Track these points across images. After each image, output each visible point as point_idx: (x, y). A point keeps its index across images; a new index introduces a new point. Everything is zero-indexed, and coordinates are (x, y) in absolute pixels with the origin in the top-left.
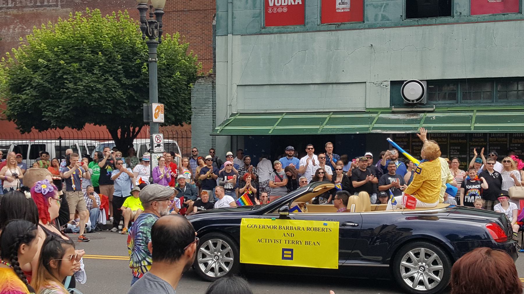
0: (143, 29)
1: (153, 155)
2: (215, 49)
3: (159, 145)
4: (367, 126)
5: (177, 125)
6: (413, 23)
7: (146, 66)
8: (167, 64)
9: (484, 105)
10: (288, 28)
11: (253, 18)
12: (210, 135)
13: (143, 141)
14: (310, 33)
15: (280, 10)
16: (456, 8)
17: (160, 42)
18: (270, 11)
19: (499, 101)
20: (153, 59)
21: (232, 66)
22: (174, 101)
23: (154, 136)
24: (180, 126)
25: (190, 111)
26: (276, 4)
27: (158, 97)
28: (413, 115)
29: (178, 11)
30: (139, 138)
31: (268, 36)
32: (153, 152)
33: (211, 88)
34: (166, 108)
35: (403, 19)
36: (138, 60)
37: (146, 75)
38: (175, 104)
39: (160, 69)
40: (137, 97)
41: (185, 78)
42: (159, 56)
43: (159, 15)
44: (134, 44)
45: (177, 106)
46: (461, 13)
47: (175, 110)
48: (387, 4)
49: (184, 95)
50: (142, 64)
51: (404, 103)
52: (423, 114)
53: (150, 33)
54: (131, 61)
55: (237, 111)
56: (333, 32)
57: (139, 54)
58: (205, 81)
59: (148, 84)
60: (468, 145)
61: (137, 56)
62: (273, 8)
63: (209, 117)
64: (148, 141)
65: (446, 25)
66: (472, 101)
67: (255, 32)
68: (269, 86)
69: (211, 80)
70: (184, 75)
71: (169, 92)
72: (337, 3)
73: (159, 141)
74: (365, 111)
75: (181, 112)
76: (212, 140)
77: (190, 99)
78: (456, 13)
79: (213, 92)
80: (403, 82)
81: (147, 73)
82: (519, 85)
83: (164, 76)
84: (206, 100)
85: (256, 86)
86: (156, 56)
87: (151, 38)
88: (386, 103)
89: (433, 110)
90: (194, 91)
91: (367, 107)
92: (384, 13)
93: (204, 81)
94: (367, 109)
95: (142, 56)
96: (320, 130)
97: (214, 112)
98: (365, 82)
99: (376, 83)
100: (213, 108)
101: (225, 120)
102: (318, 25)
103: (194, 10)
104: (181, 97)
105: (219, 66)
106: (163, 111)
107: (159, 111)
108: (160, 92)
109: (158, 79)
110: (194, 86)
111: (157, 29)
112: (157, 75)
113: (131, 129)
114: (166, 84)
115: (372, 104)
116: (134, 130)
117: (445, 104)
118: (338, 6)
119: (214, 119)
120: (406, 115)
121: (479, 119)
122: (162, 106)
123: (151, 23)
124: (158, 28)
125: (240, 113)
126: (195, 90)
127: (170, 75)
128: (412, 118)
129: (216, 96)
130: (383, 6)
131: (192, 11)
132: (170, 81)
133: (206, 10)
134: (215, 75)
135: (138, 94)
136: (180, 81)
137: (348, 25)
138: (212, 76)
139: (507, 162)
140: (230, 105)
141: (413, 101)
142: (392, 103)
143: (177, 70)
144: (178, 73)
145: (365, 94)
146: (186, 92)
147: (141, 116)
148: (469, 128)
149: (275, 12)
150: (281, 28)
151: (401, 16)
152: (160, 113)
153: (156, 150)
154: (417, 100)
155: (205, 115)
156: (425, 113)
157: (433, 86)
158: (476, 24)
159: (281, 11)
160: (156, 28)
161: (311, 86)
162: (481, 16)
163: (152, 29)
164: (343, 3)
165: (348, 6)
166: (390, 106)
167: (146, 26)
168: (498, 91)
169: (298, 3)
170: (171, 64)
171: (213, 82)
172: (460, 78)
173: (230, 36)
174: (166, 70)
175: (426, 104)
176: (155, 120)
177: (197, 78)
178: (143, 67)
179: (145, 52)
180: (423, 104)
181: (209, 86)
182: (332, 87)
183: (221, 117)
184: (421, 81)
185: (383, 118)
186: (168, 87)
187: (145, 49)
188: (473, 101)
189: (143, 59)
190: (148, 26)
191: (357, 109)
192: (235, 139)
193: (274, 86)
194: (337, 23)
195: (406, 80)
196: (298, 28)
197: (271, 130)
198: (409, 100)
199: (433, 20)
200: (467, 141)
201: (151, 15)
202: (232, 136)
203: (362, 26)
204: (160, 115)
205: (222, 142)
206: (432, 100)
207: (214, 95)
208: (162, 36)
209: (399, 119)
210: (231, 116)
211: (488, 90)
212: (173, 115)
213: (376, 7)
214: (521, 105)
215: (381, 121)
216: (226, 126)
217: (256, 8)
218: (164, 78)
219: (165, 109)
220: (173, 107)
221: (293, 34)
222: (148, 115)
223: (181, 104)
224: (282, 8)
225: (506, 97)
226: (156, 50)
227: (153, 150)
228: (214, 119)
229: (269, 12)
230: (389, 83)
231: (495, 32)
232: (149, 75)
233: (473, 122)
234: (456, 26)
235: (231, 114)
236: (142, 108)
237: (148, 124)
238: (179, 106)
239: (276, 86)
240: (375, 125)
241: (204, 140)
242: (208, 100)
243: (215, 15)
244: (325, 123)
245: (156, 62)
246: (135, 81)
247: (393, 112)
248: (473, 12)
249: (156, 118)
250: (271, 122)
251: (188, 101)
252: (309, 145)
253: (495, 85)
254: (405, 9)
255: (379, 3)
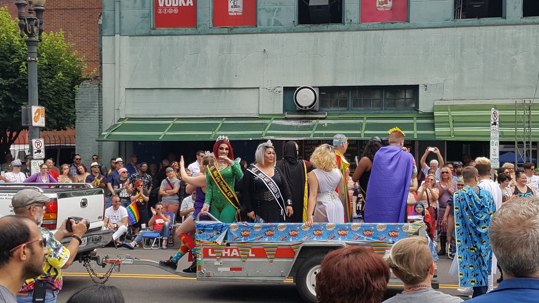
0: (21, 26)
1: (32, 161)
2: (101, 50)
3: (39, 151)
4: (260, 132)
5: (59, 130)
6: (305, 29)
7: (25, 66)
8: (48, 64)
9: (374, 113)
10: (179, 30)
11: (142, 18)
12: (96, 141)
13: (22, 147)
14: (203, 36)
15: (170, 11)
16: (347, 14)
17: (40, 40)
18: (160, 11)
19: (388, 108)
20: (33, 58)
21: (120, 69)
22: (56, 104)
23: (34, 141)
24: (62, 130)
25: (74, 115)
26: (167, 5)
27: (38, 98)
28: (305, 121)
29: (60, 9)
30: (17, 144)
31: (158, 37)
32: (33, 159)
33: (98, 91)
34: (47, 111)
35: (296, 25)
36: (16, 59)
37: (25, 75)
38: (57, 107)
39: (40, 69)
40: (15, 99)
41: (68, 79)
42: (39, 55)
43: (39, 12)
44: (12, 42)
45: (60, 109)
46: (351, 20)
47: (58, 114)
48: (280, 9)
49: (67, 97)
50: (20, 63)
51: (297, 109)
52: (315, 121)
53: (30, 31)
54: (8, 61)
55: (126, 116)
56: (226, 36)
57: (18, 53)
58: (91, 83)
59: (27, 85)
60: (359, 152)
61: (15, 55)
62: (163, 9)
63: (95, 121)
64: (27, 147)
65: (337, 33)
66: (362, 109)
67: (144, 32)
68: (159, 90)
69: (97, 82)
70: (68, 77)
71: (51, 94)
72: (230, 6)
73: (39, 147)
74: (258, 117)
75: (64, 116)
76: (98, 146)
77: (74, 102)
78: (347, 20)
79: (99, 95)
80: (296, 88)
81: (26, 73)
82: (406, 94)
83: (45, 77)
84: (92, 103)
85: (145, 90)
86: (36, 55)
87: (30, 36)
88: (279, 109)
89: (325, 117)
90: (78, 94)
91: (260, 113)
92: (277, 18)
93: (89, 84)
94: (260, 115)
95: (20, 55)
96: (213, 136)
97: (100, 116)
98: (259, 88)
99: (269, 89)
100: (99, 113)
101: (113, 125)
102: (210, 28)
103: (78, 9)
104: (63, 99)
105: (106, 68)
106: (44, 114)
107: (39, 115)
108: (41, 94)
109: (38, 80)
110: (79, 88)
111: (37, 26)
112: (37, 75)
113: (8, 133)
114: (48, 86)
115: (265, 110)
116: (11, 135)
117: (337, 111)
118: (230, 9)
119: (101, 124)
120: (299, 121)
121: (369, 127)
122: (42, 109)
123: (30, 20)
124: (38, 26)
125: (129, 118)
126: (80, 92)
127: (52, 75)
128: (304, 124)
129: (102, 100)
130: (275, 12)
131: (76, 9)
132: (51, 82)
133: (92, 9)
134: (102, 77)
135: (16, 96)
136: (62, 82)
137: (240, 29)
138: (99, 78)
139: (126, 173)
140: (118, 109)
141: (306, 107)
142: (285, 110)
143: (59, 70)
144: (60, 74)
145: (258, 99)
146: (70, 95)
147: (20, 119)
148: (359, 135)
149: (165, 13)
150: (172, 30)
151: (294, 21)
152: (40, 116)
153: (35, 156)
154: (310, 107)
155: (91, 119)
156: (318, 120)
157: (325, 93)
158: (366, 31)
159: (172, 12)
160: (36, 25)
161: (204, 91)
162: (370, 25)
163: (32, 26)
164: (236, 6)
165: (241, 9)
166: (283, 112)
167: (24, 23)
168: (387, 99)
169: (190, 4)
170: (52, 64)
171: (99, 85)
172: (351, 85)
173: (117, 36)
174: (48, 71)
175: (319, 111)
176: (34, 124)
177: (82, 80)
178: (21, 67)
179: (23, 50)
180: (315, 111)
181: (95, 88)
182: (225, 92)
183: (108, 122)
184: (313, 87)
185: (276, 124)
186: (49, 88)
187: (23, 47)
188: (363, 108)
189: (21, 58)
190: (27, 22)
191: (250, 115)
192: (123, 145)
193: (165, 90)
194: (230, 27)
195: (299, 86)
196: (190, 30)
197: (161, 135)
198: (302, 107)
199: (325, 27)
200: (357, 148)
201: (30, 12)
202: (120, 142)
203: (255, 30)
204: (40, 118)
205: (109, 148)
206: (324, 107)
207: (100, 98)
208: (43, 33)
209: (291, 126)
210: (119, 121)
211: (378, 98)
212: (54, 118)
213: (269, 11)
214: (408, 113)
215: (274, 127)
216: (113, 131)
217: (144, 7)
218: (45, 79)
219: (46, 112)
220: (55, 111)
221: (184, 36)
222: (27, 119)
223: (64, 107)
224: (173, 9)
225: (395, 105)
226: (35, 49)
227: (33, 156)
228: (101, 124)
229: (159, 12)
230: (282, 89)
231: (384, 41)
232: (27, 75)
233: (363, 129)
234: (346, 33)
235: (119, 118)
236: (20, 111)
237: (27, 128)
238: (62, 109)
239: (167, 90)
240: (268, 131)
241: (89, 146)
242: (94, 103)
243: (101, 13)
244: (217, 129)
245: (35, 61)
246: (12, 81)
247: (286, 119)
248: (363, 19)
249: (36, 121)
250: (162, 128)
251: (71, 104)
252: (202, 152)
253: (384, 93)
254: (297, 15)
255: (272, 8)
